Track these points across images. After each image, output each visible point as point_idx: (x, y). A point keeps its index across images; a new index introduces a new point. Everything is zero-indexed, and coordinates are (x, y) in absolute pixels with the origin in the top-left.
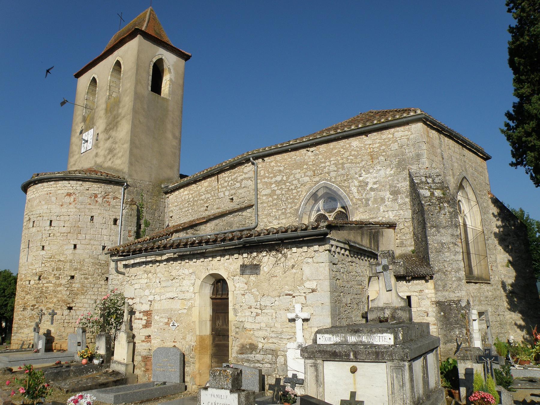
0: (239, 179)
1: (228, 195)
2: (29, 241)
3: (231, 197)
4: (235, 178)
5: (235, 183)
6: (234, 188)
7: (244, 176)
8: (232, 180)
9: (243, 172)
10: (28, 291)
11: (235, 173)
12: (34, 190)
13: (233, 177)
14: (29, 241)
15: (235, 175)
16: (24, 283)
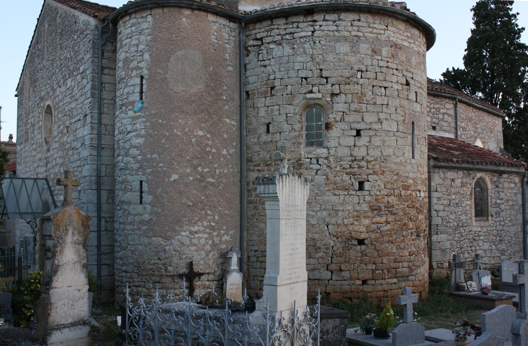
0: (442, 111)
1: (431, 122)
2: (413, 123)
3: (434, 125)
4: (437, 108)
5: (438, 113)
6: (437, 119)
7: (445, 111)
8: (434, 108)
9: (445, 107)
10: (419, 207)
11: (437, 103)
12: (409, 35)
13: (436, 106)
14: (413, 123)
15: (438, 106)
16: (414, 193)
